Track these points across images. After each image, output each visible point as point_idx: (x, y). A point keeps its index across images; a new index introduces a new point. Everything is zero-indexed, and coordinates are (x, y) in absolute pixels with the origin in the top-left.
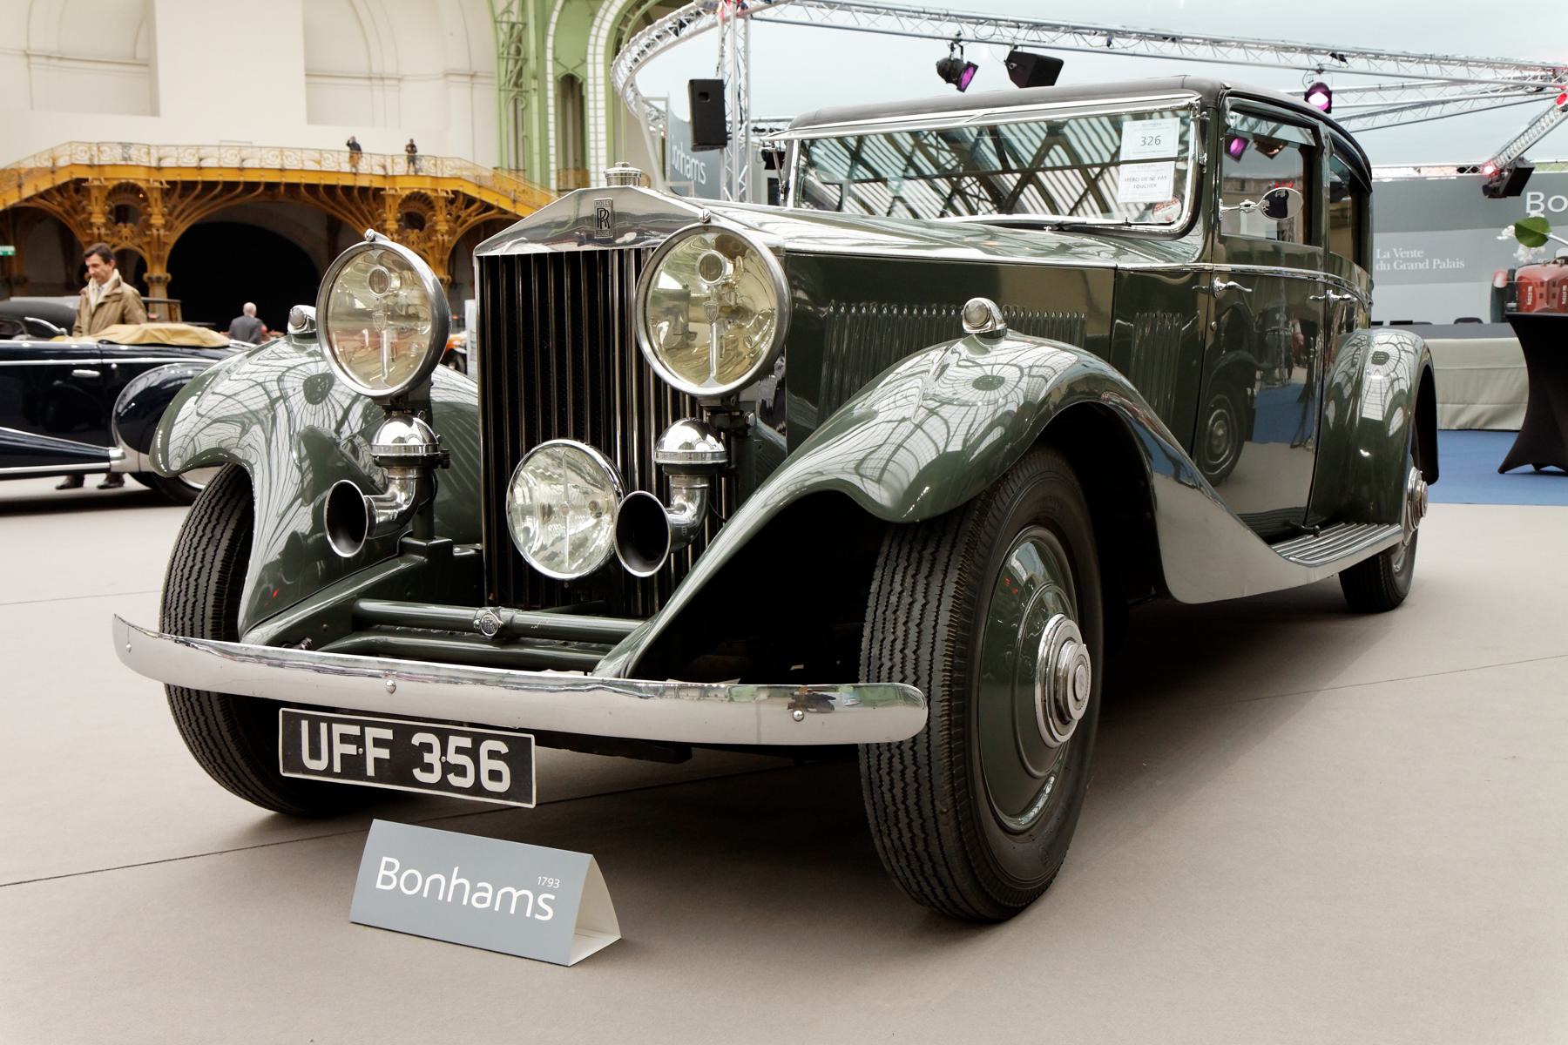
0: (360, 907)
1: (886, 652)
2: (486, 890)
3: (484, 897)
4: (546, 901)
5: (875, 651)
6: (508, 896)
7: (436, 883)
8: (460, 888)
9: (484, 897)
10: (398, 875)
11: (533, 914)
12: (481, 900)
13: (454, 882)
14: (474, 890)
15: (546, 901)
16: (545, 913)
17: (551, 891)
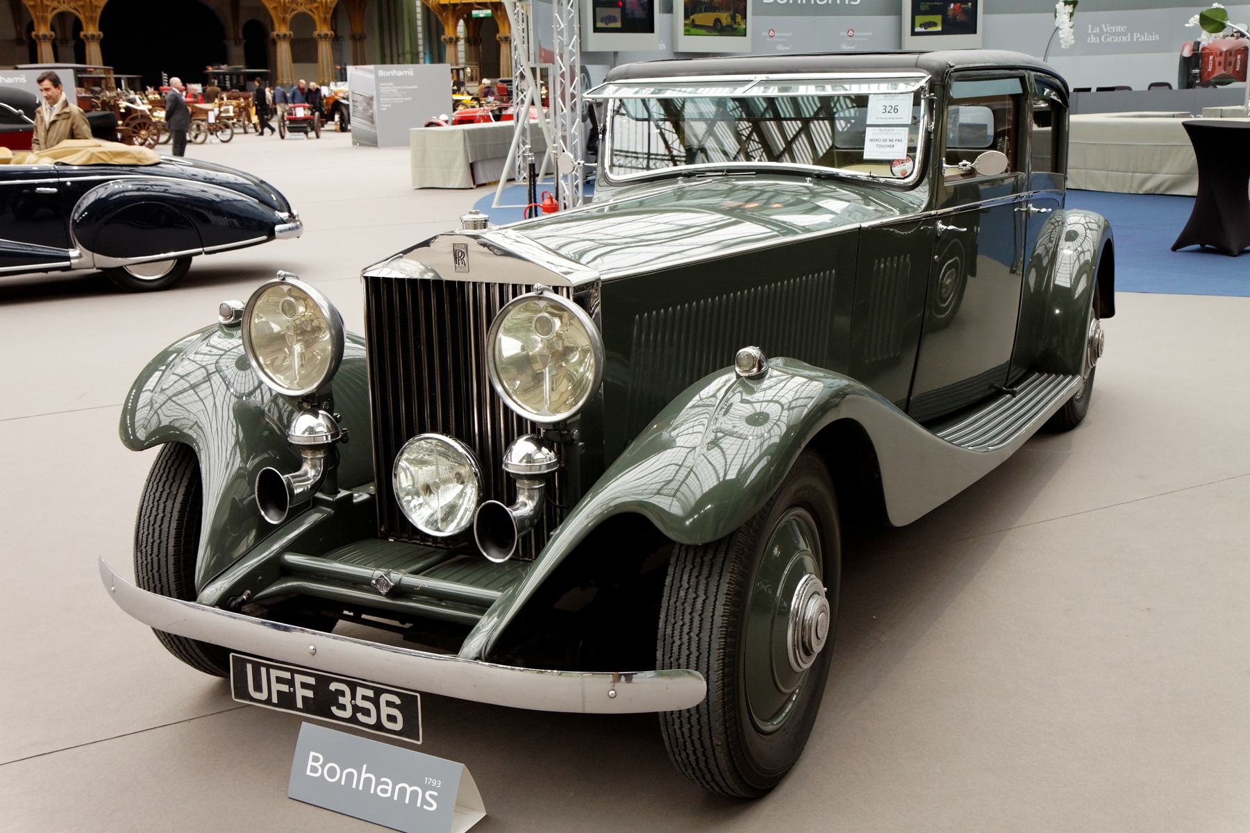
0: (295, 789)
1: (677, 633)
2: (387, 784)
3: (386, 789)
4: (431, 796)
5: (669, 631)
6: (403, 790)
7: (350, 776)
8: (368, 781)
9: (386, 789)
10: (323, 766)
13: (364, 775)
14: (378, 784)
15: (431, 796)
16: (431, 805)
17: (434, 789)
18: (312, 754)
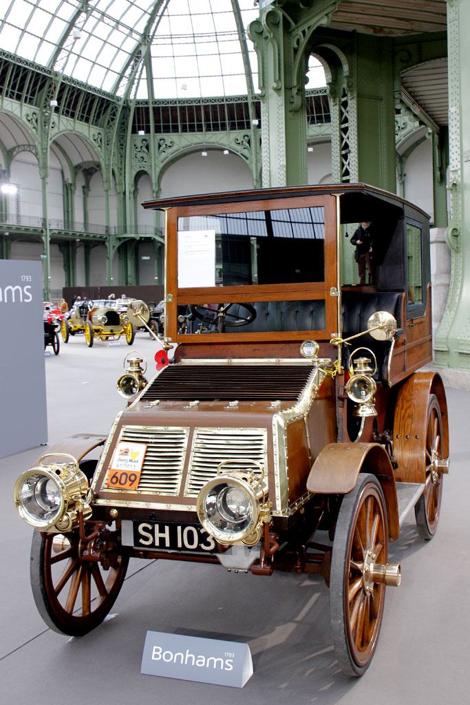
4: (28, 290)
6: (10, 291)
11: (23, 300)
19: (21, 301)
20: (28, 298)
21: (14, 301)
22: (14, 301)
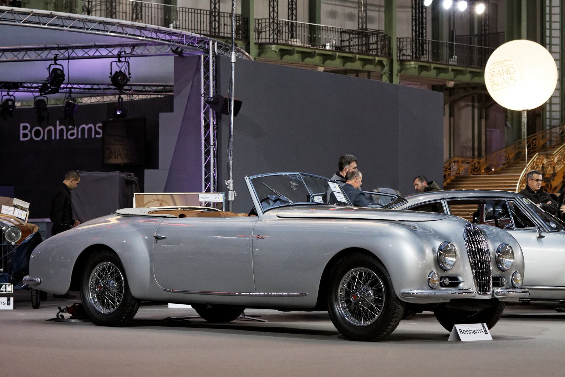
2: (73, 129)
4: (99, 127)
6: (83, 129)
7: (50, 131)
10: (31, 131)
11: (95, 136)
12: (72, 134)
13: (58, 128)
14: (68, 130)
15: (99, 127)
18: (22, 125)
19: (93, 136)
20: (99, 134)
21: (86, 137)
22: (86, 137)
